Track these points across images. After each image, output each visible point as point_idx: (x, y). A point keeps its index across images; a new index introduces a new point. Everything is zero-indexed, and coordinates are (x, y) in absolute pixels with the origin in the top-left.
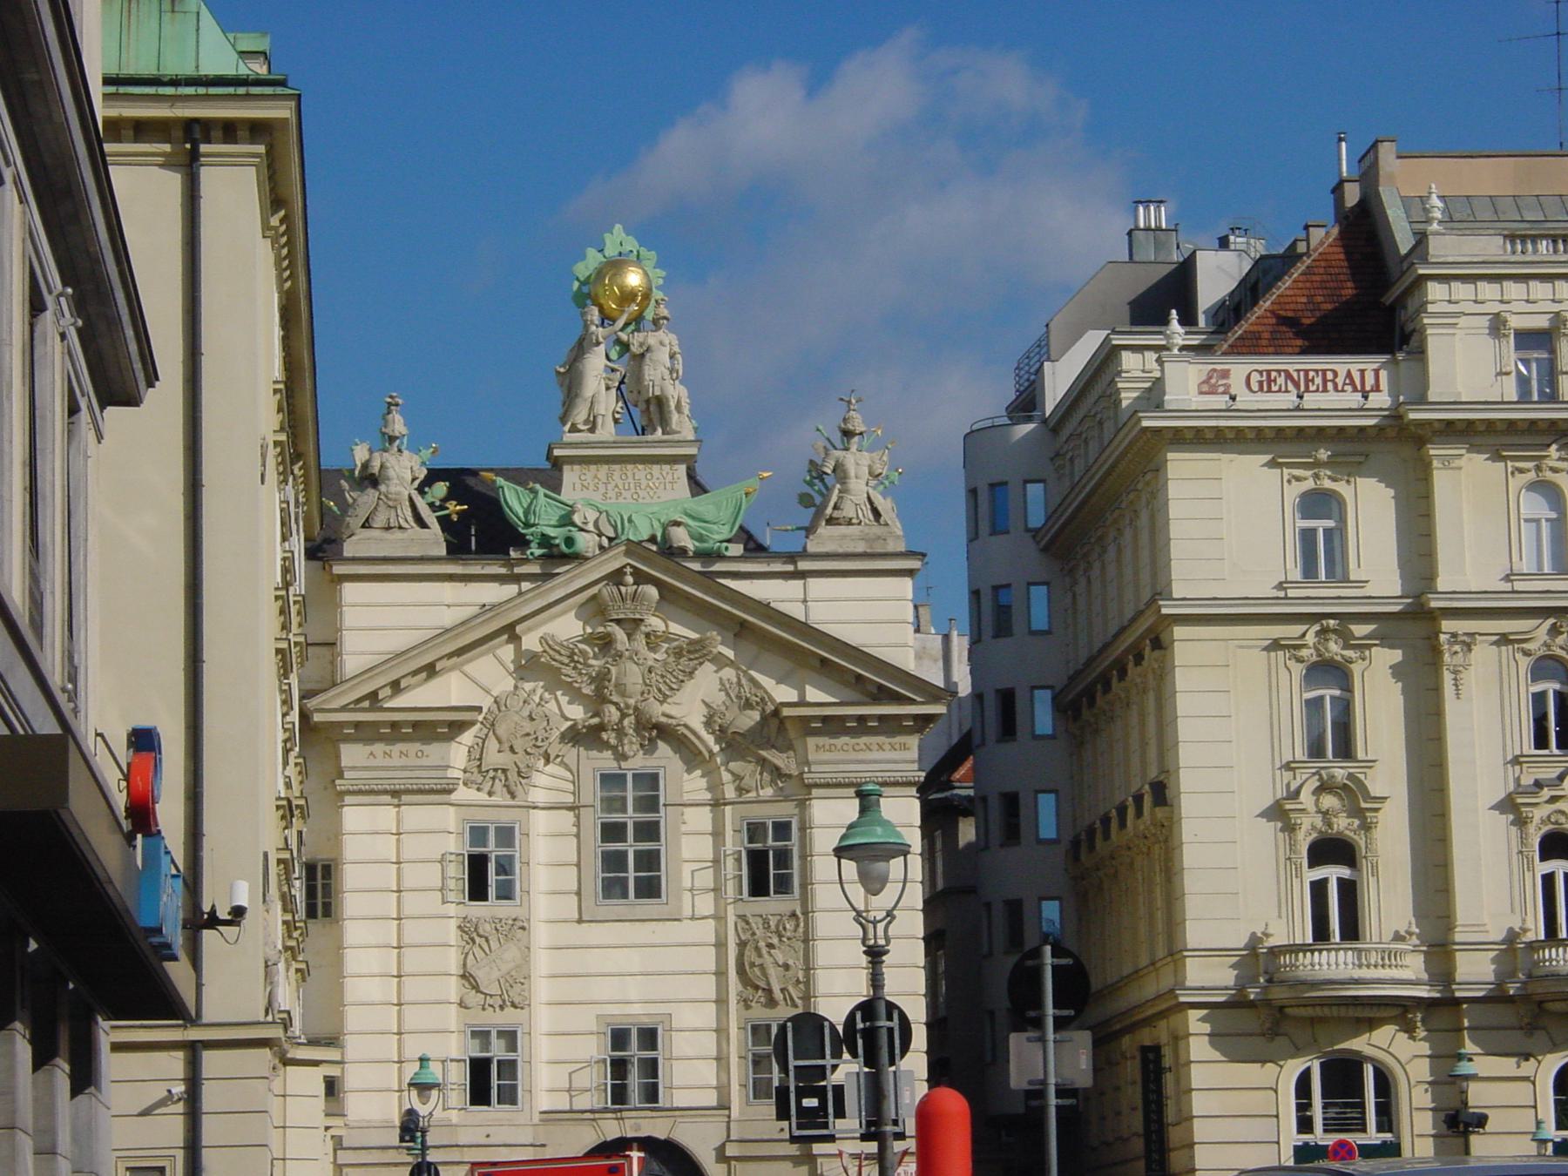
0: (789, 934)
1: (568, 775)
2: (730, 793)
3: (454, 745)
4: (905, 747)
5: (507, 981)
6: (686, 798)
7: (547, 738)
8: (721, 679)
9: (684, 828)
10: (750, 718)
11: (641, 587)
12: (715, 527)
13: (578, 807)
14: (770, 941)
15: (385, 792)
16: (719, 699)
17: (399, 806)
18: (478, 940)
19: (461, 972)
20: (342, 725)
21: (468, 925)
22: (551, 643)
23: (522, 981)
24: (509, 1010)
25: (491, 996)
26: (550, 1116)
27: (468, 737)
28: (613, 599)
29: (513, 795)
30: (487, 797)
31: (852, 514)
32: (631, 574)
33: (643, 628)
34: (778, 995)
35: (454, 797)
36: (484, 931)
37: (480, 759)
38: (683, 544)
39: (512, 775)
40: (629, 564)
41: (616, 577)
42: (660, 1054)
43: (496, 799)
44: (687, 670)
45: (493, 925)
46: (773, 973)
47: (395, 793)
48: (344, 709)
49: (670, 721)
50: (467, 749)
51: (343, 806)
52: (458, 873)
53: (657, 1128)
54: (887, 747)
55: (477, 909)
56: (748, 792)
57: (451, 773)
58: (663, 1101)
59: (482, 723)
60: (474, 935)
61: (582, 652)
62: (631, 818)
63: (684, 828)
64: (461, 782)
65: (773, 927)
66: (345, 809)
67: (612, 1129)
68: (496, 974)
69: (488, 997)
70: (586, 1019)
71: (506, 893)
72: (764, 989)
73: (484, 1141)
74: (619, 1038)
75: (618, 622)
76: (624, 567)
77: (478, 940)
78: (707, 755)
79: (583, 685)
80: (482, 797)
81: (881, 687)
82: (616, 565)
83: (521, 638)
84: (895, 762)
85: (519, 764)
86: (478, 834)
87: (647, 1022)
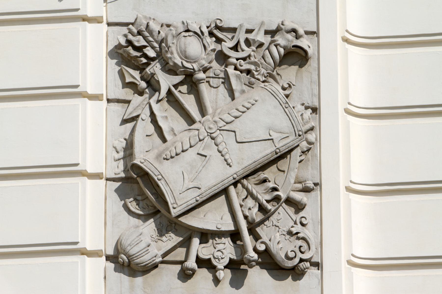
5: (250, 194)
21: (139, 41)
23: (298, 196)
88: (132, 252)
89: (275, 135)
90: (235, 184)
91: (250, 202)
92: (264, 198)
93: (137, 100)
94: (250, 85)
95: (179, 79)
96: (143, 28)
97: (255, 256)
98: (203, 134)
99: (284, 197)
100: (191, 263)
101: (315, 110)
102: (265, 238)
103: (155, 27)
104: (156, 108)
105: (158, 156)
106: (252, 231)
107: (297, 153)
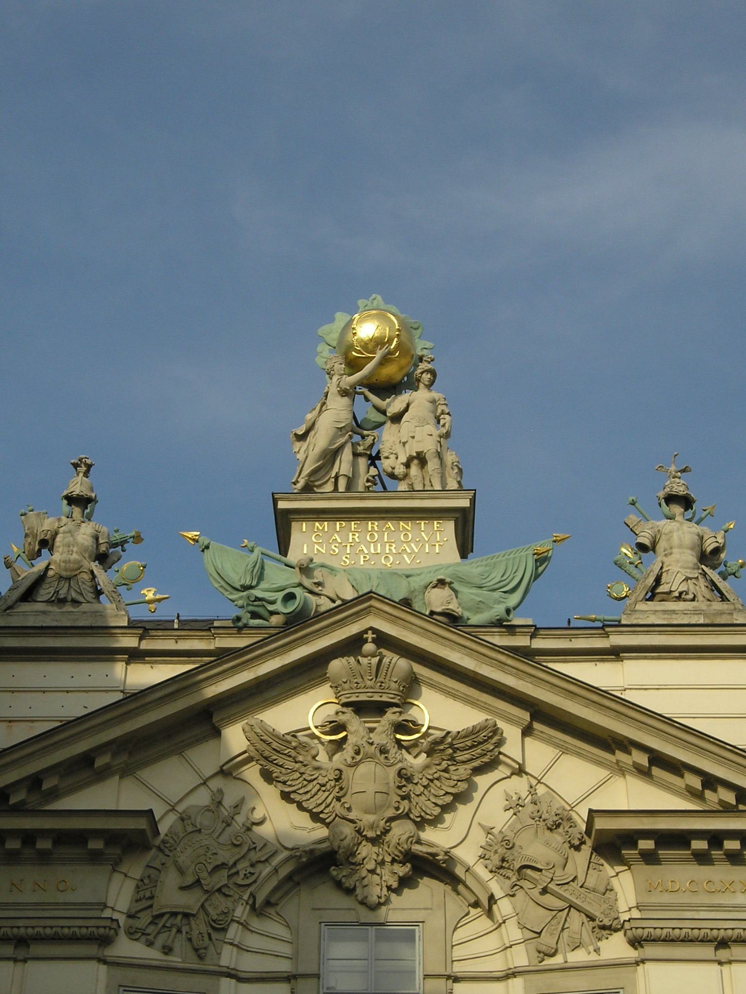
3: (117, 878)
6: (458, 968)
7: (253, 874)
8: (507, 794)
10: (547, 844)
12: (497, 594)
17: (25, 961)
27: (136, 869)
29: (201, 958)
32: (374, 641)
33: (391, 716)
37: (152, 898)
38: (451, 607)
40: (371, 628)
43: (175, 960)
47: (22, 942)
49: (430, 850)
50: (136, 882)
57: (107, 913)
76: (365, 631)
79: (309, 796)
80: (153, 955)
82: (353, 629)
85: (210, 909)
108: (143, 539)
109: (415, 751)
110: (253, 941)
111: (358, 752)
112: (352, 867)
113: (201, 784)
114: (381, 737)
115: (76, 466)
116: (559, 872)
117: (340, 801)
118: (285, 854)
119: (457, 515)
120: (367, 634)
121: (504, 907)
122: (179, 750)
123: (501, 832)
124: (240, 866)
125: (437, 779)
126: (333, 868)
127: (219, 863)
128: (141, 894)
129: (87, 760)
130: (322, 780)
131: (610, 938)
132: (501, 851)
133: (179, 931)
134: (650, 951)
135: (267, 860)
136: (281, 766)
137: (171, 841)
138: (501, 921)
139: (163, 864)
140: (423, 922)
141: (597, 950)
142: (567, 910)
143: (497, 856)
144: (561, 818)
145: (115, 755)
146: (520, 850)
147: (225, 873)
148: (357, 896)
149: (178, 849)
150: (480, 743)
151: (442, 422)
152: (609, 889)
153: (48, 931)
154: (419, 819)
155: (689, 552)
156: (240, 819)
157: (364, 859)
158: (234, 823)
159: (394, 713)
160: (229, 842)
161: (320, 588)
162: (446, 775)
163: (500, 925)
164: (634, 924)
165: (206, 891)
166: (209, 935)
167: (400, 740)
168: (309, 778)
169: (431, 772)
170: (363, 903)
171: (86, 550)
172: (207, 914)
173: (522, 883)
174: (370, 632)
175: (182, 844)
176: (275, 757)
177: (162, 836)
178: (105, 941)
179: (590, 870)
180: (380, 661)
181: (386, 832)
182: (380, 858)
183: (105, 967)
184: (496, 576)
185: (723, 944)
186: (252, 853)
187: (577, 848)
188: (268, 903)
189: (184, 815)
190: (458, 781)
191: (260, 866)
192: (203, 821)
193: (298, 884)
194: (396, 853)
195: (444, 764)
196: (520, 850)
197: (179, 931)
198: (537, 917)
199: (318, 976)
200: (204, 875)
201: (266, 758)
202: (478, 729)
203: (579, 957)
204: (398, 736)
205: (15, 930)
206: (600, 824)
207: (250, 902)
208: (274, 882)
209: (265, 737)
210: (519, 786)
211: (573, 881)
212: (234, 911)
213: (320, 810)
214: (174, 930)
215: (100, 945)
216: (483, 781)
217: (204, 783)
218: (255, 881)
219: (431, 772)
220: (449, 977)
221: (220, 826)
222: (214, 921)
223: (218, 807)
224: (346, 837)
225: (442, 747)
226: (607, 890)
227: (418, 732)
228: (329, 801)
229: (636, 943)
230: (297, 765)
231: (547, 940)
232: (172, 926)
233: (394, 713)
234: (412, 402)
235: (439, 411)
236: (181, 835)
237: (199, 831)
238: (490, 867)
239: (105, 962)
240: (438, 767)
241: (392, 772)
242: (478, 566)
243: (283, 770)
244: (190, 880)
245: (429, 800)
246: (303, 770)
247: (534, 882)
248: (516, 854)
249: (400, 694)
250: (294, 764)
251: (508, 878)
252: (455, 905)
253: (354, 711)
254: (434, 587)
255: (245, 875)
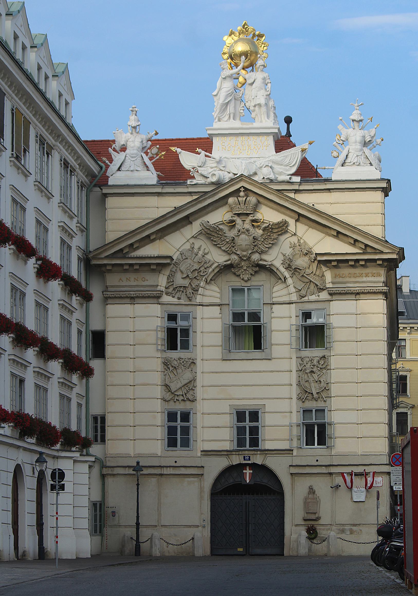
0: (320, 366)
1: (217, 289)
2: (294, 298)
3: (161, 276)
4: (379, 275)
6: (274, 300)
9: (273, 315)
11: (248, 199)
12: (288, 168)
13: (221, 305)
14: (312, 370)
15: (127, 297)
16: (288, 251)
17: (134, 304)
18: (171, 369)
19: (163, 384)
20: (105, 265)
22: (205, 225)
23: (193, 388)
24: (188, 402)
25: (177, 395)
26: (206, 453)
27: (167, 272)
28: (235, 204)
29: (190, 300)
30: (177, 300)
31: (355, 161)
33: (250, 218)
34: (315, 396)
35: (161, 300)
36: (174, 364)
37: (173, 281)
39: (190, 290)
40: (243, 186)
41: (236, 193)
42: (260, 424)
43: (182, 301)
44: (272, 238)
45: (179, 361)
46: (313, 384)
47: (132, 298)
48: (107, 257)
51: (107, 304)
52: (163, 335)
53: (258, 460)
54: (370, 275)
55: (174, 355)
56: (304, 297)
57: (159, 288)
58: (262, 446)
59: (174, 264)
60: (170, 366)
61: (221, 230)
62: (246, 310)
63: (273, 315)
64: (164, 293)
65: (315, 362)
66: (109, 306)
67: (236, 460)
68: (179, 385)
69: (176, 396)
70: (225, 407)
71: (185, 346)
72: (309, 393)
73: (175, 464)
74: (240, 416)
75: (239, 215)
76: (241, 188)
77: (171, 369)
78: (283, 280)
79: (223, 245)
80: (175, 300)
81: (366, 246)
83: (192, 223)
84: (375, 282)
85: (192, 284)
86: (172, 317)
87: (253, 408)
88: (165, 398)
89: (189, 378)
90: (183, 387)
91: (185, 390)
92: (187, 389)
93: (166, 372)
94: (186, 369)
95: (173, 368)
96: (167, 359)
97: (186, 399)
98: (177, 378)
99: (191, 388)
100: (175, 400)
101: (196, 373)
102: (187, 396)
103: (169, 359)
104: (169, 373)
105: (170, 382)
106: (185, 394)
107: (193, 381)
108: (158, 133)
109: (260, 228)
110: (207, 293)
111: (239, 231)
112: (239, 268)
113: (187, 241)
114: (247, 225)
115: (132, 111)
116: (307, 270)
117: (234, 247)
118: (216, 265)
119: (274, 134)
120: (241, 188)
121: (290, 281)
122: (178, 229)
123: (288, 255)
124: (201, 269)
125: (267, 239)
126: (232, 269)
127: (194, 269)
128: (169, 281)
129: (148, 236)
130: (227, 240)
131: (323, 292)
132: (288, 262)
133: (183, 292)
134: (335, 297)
135: (210, 266)
136: (214, 236)
137: (178, 262)
138: (288, 285)
139: (176, 270)
140: (263, 285)
141: (319, 296)
142: (309, 283)
143: (287, 264)
144: (308, 252)
145: (156, 234)
146: (294, 262)
147: (197, 272)
148: (240, 277)
149: (180, 265)
150: (280, 227)
151: (267, 90)
152: (323, 276)
153: (140, 295)
154: (261, 252)
155: (358, 144)
156: (201, 253)
157: (242, 266)
158: (198, 254)
159: (252, 216)
160: (197, 261)
161: (224, 168)
162: (270, 237)
163: (288, 286)
164: (329, 289)
165: (191, 279)
166: (193, 293)
167: (254, 225)
168: (223, 239)
169: (264, 236)
170: (243, 279)
171: (139, 148)
172: (192, 286)
173: (295, 273)
174: (242, 188)
175: (182, 263)
176: (211, 233)
177: (175, 260)
178: (159, 297)
179: (318, 269)
180: (246, 199)
181: (249, 258)
182: (248, 265)
183: (160, 306)
184: (287, 161)
185: (358, 294)
186: (205, 264)
187: (314, 262)
188: (211, 280)
189: (181, 253)
190: (274, 239)
191: (208, 269)
192: (188, 254)
193: (221, 273)
194: (253, 264)
195: (269, 234)
196: (294, 262)
197: (183, 292)
198: (300, 285)
199: (229, 304)
200: (189, 273)
201: (208, 234)
202: (280, 223)
203: (313, 298)
204: (253, 224)
205: (130, 295)
206: (319, 258)
207: (206, 280)
208: (213, 274)
209: (208, 227)
210: (294, 240)
211: (311, 273)
212: (200, 284)
213: (227, 250)
214: (181, 292)
215: (157, 298)
216: (282, 238)
217: (188, 240)
218: (207, 274)
219: (264, 236)
220: (271, 304)
221: (194, 255)
222: (193, 288)
223: (193, 249)
224: (236, 260)
225: (268, 229)
226: (322, 276)
227: (260, 222)
228: (230, 247)
229: (331, 294)
230: (219, 236)
231: (303, 292)
232: (180, 291)
233: (252, 216)
234: (256, 79)
235: (267, 82)
236: (181, 260)
237: (187, 258)
238: (285, 267)
239: (160, 304)
240: (267, 235)
241: (251, 238)
242: (281, 157)
243: (214, 237)
244: (185, 276)
245: (264, 245)
246: (221, 237)
247: (299, 273)
248: (293, 263)
249: (253, 210)
250: (217, 235)
251: (291, 271)
252: (273, 280)
253: (237, 216)
254: (265, 167)
255: (203, 272)
